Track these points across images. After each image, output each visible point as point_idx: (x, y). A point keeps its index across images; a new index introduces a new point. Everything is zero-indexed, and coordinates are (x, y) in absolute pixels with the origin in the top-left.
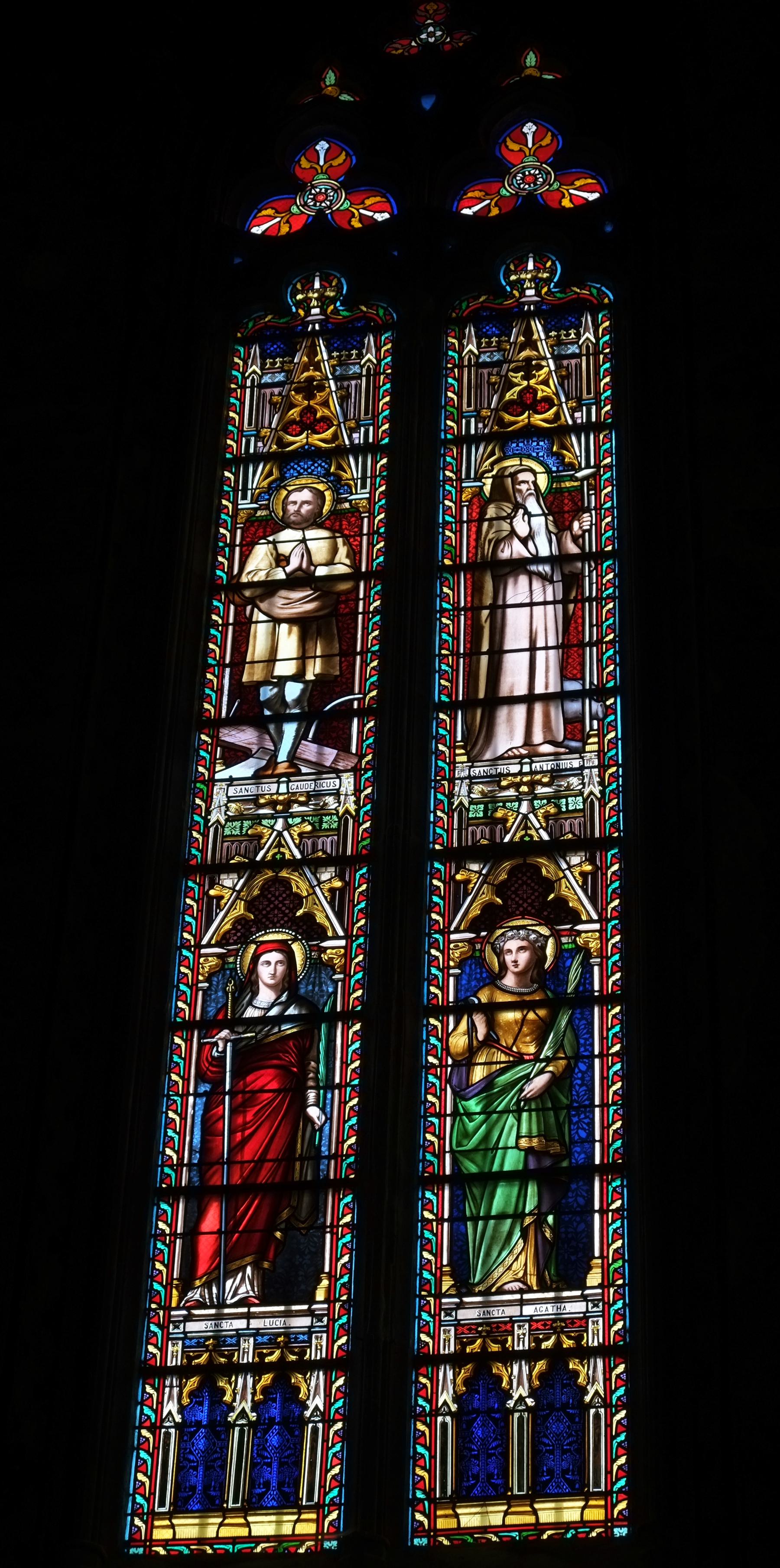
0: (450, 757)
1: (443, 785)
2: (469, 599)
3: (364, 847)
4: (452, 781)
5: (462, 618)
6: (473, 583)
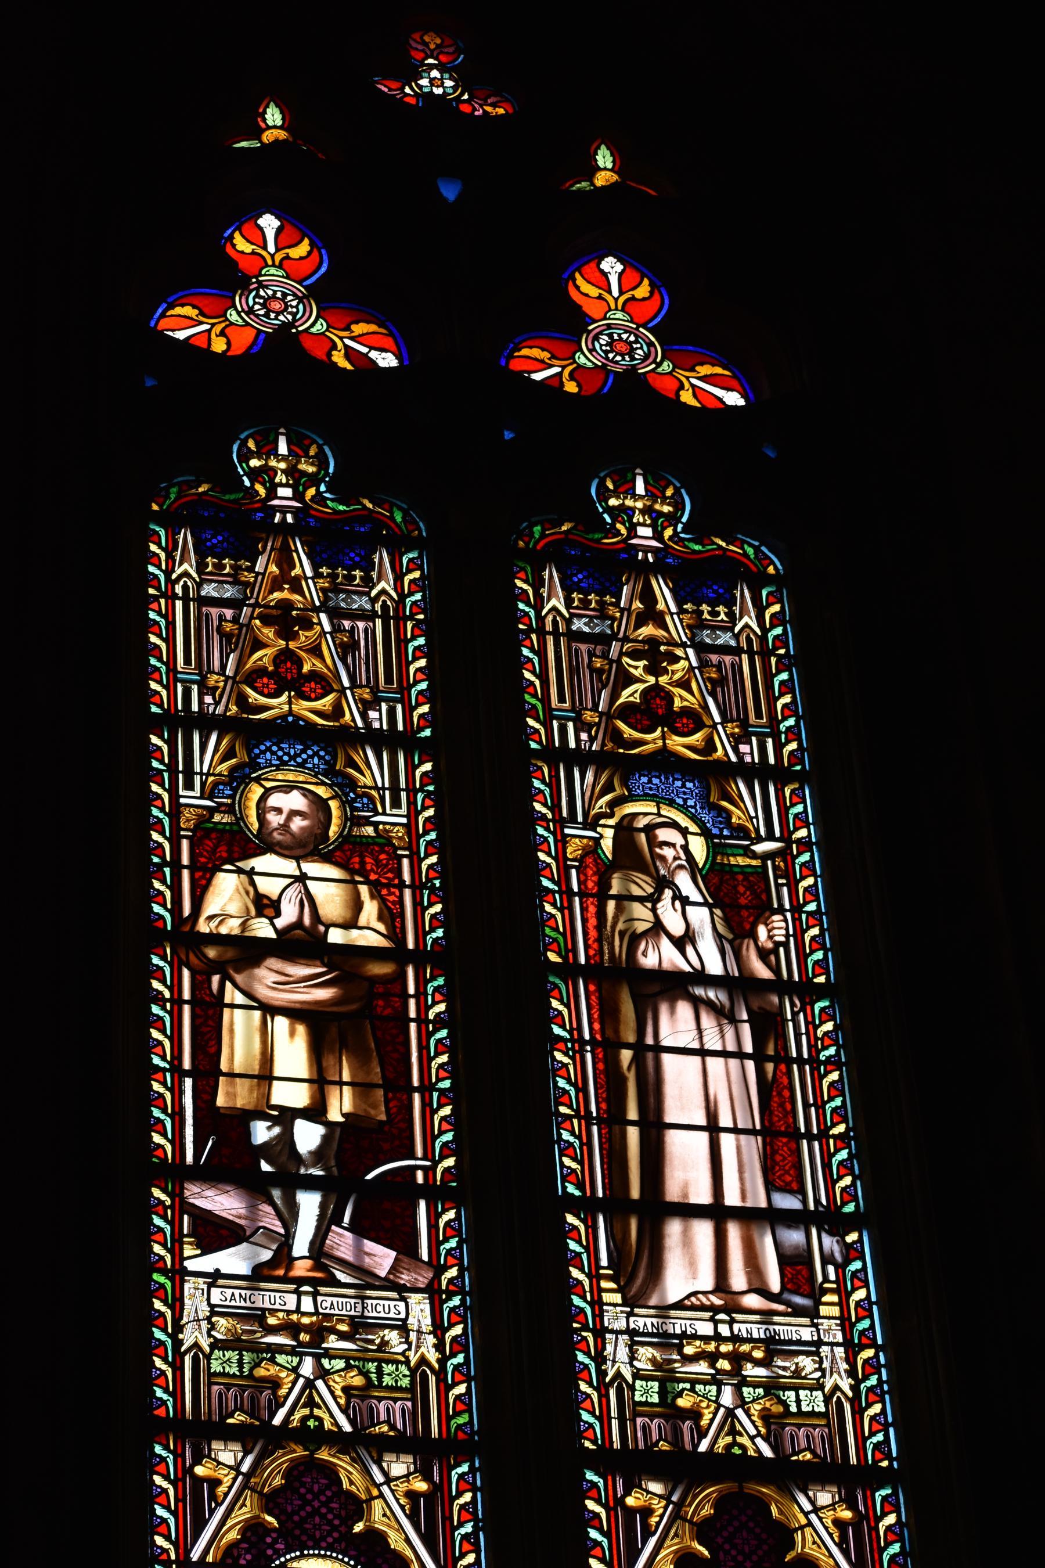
0: (591, 1291)
1: (585, 1338)
2: (597, 1026)
3: (459, 1427)
4: (600, 1332)
5: (589, 1056)
6: (600, 999)
